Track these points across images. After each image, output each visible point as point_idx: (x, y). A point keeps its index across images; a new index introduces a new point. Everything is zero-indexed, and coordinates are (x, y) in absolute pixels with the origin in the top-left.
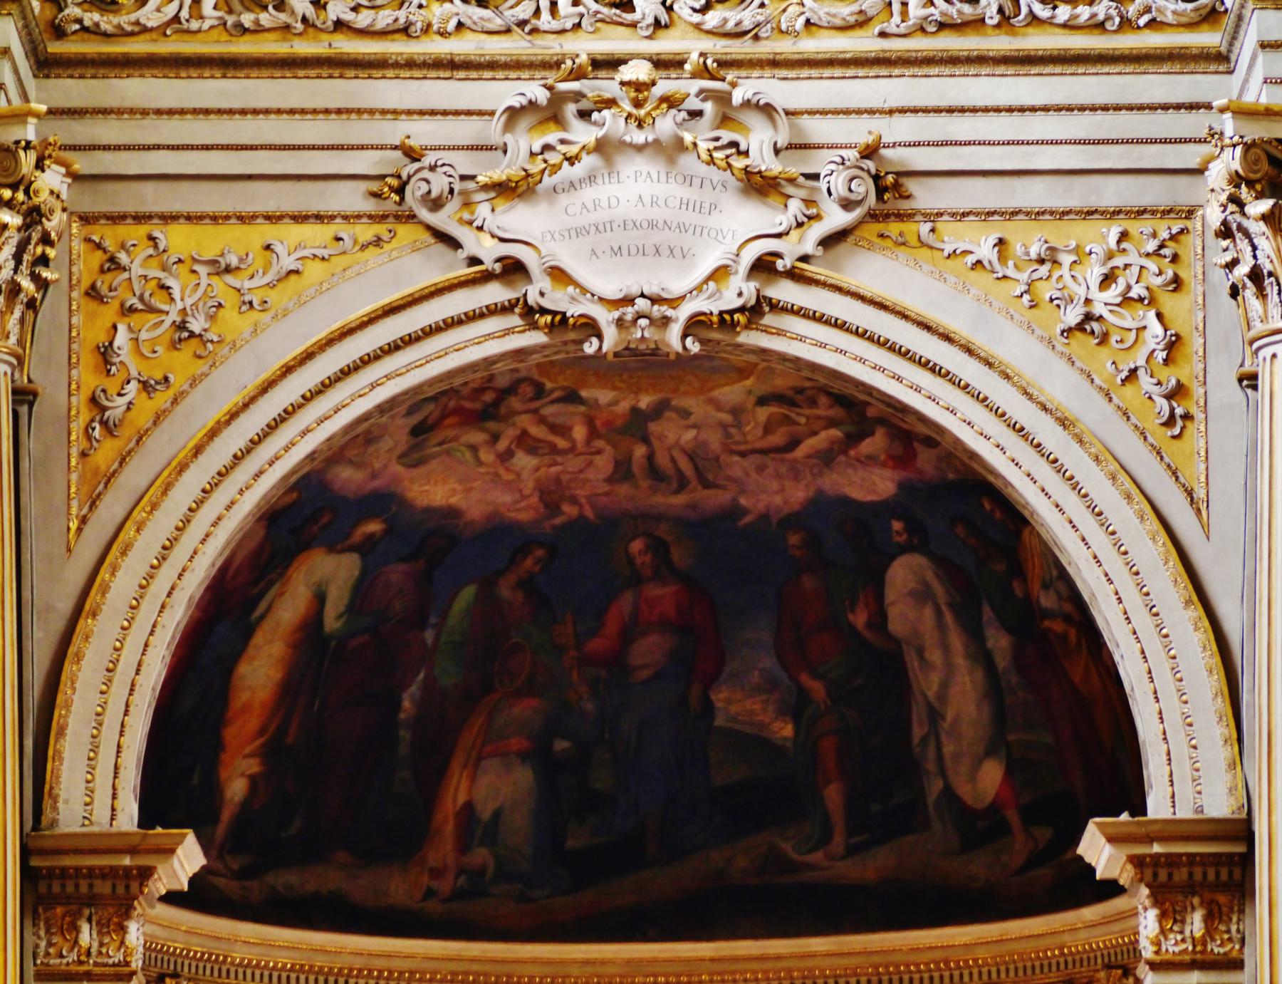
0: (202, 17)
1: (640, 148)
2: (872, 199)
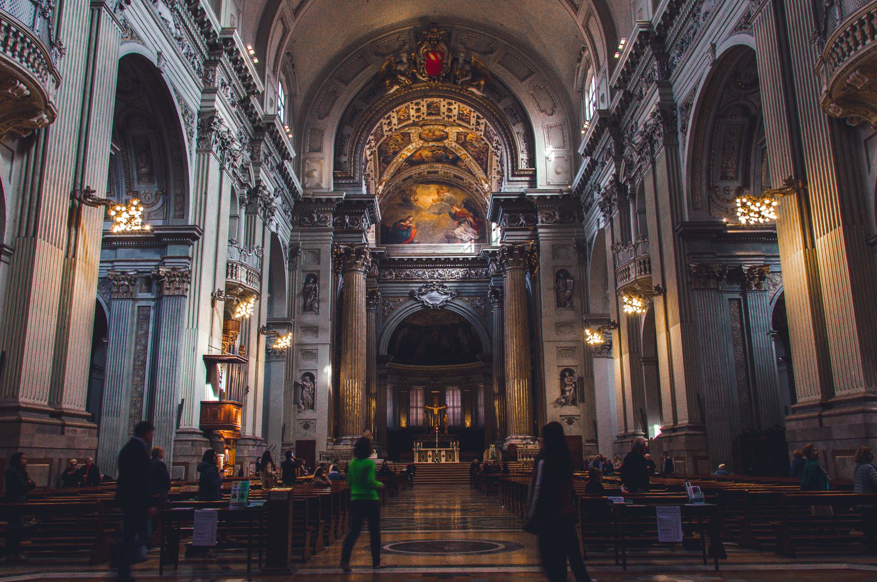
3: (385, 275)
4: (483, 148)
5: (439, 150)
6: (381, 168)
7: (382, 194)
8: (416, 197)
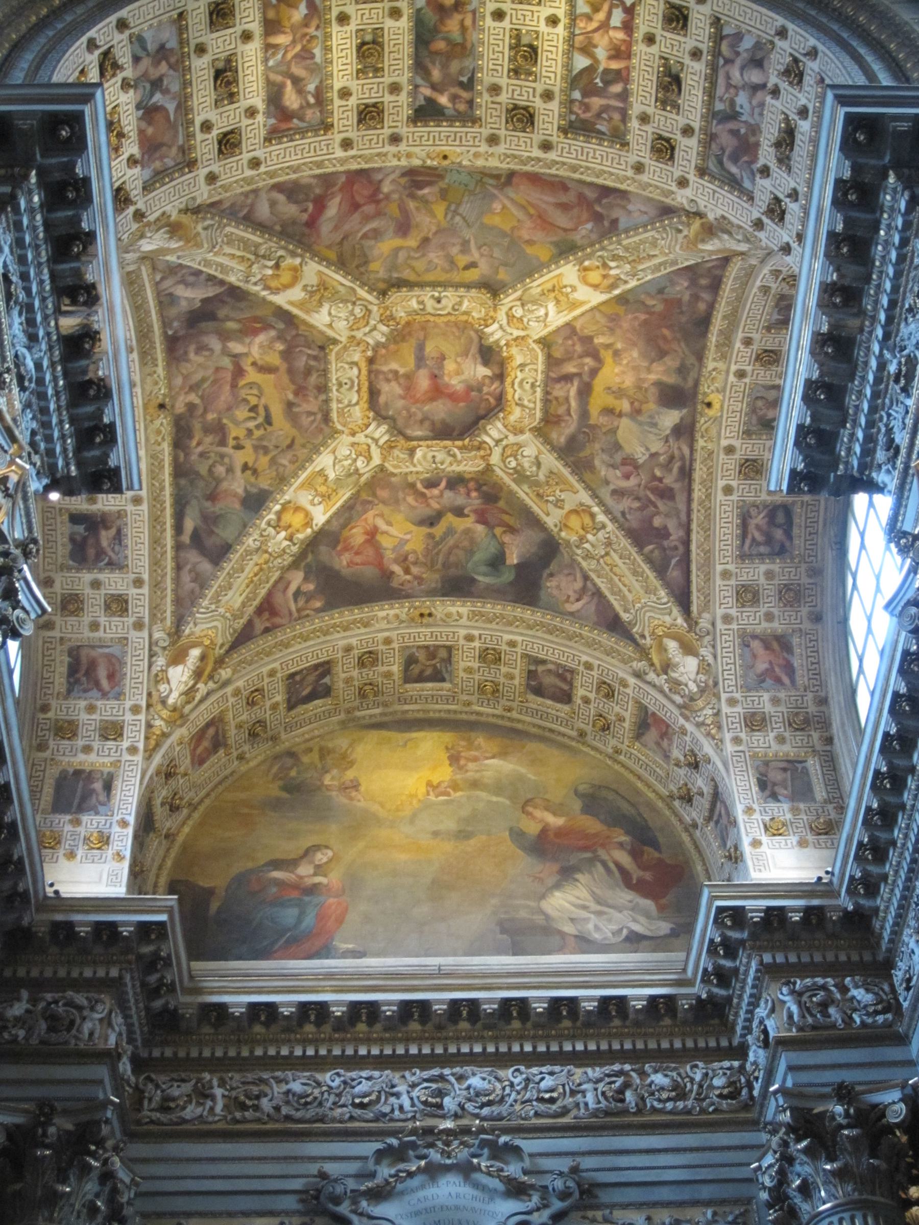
0: (215, 1115)
1: (448, 1169)
2: (577, 1195)
3: (167, 1099)
4: (667, 466)
5: (459, 512)
6: (186, 577)
7: (178, 716)
8: (350, 774)
